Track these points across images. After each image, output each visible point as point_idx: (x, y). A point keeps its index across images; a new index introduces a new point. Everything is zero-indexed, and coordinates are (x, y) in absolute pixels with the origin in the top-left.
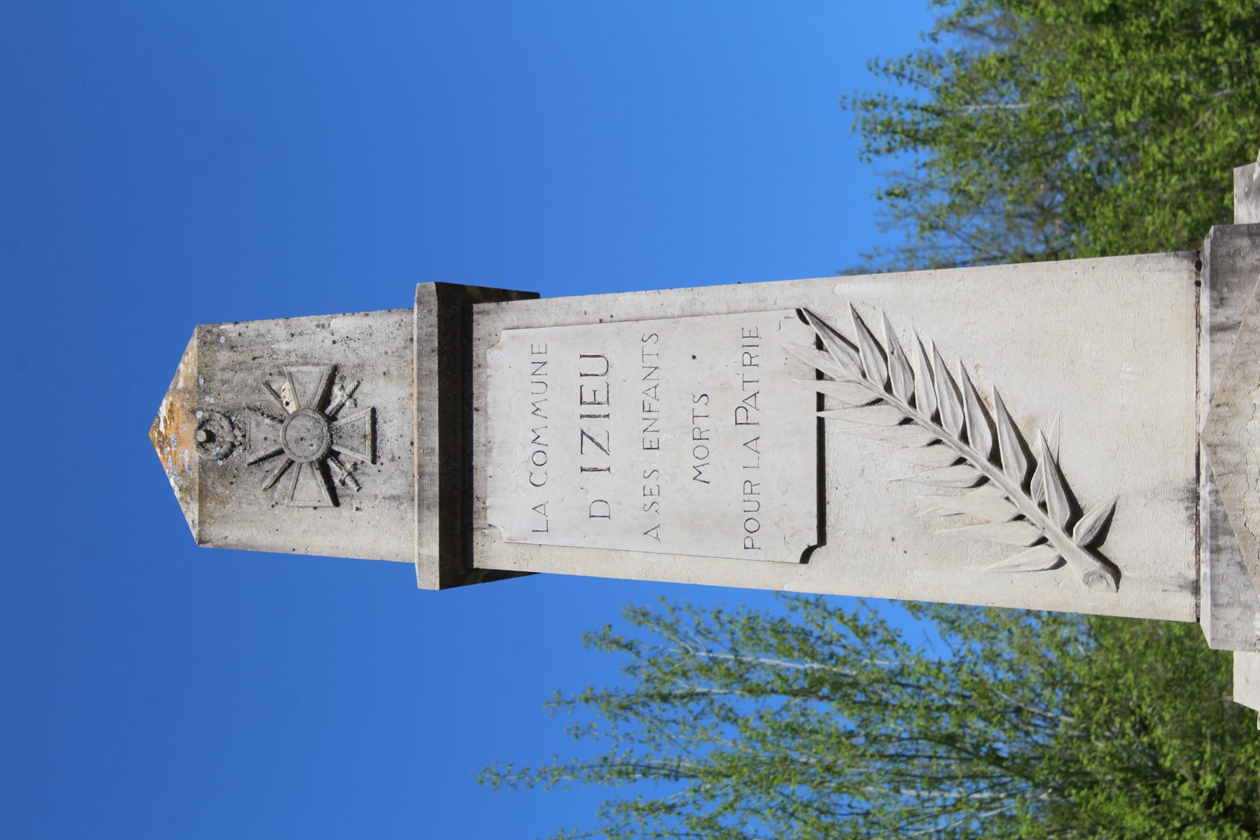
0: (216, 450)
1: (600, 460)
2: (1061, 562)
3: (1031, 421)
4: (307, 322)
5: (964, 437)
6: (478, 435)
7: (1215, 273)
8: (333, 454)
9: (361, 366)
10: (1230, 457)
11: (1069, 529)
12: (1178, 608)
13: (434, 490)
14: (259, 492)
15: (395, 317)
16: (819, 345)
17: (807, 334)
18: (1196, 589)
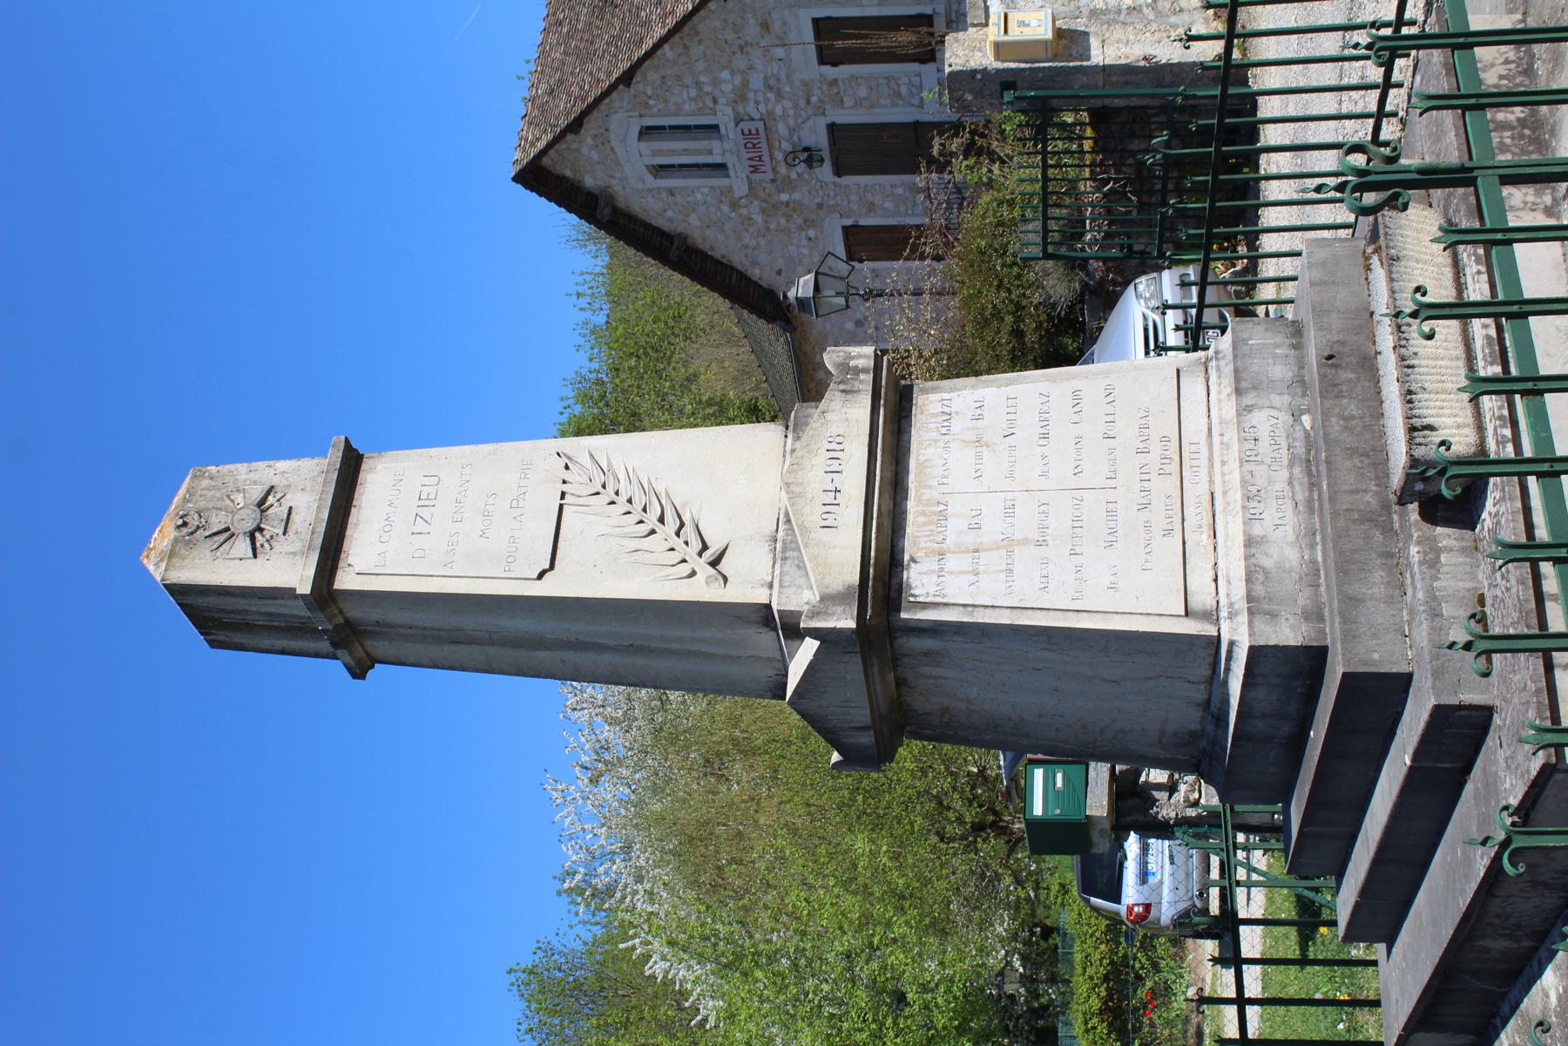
0: (185, 530)
1: (426, 528)
2: (693, 574)
3: (684, 505)
4: (261, 465)
5: (645, 510)
6: (352, 519)
7: (796, 425)
8: (261, 530)
9: (289, 486)
10: (796, 489)
11: (700, 554)
12: (761, 597)
13: (319, 540)
14: (208, 553)
15: (316, 461)
16: (567, 467)
17: (561, 462)
18: (771, 586)
